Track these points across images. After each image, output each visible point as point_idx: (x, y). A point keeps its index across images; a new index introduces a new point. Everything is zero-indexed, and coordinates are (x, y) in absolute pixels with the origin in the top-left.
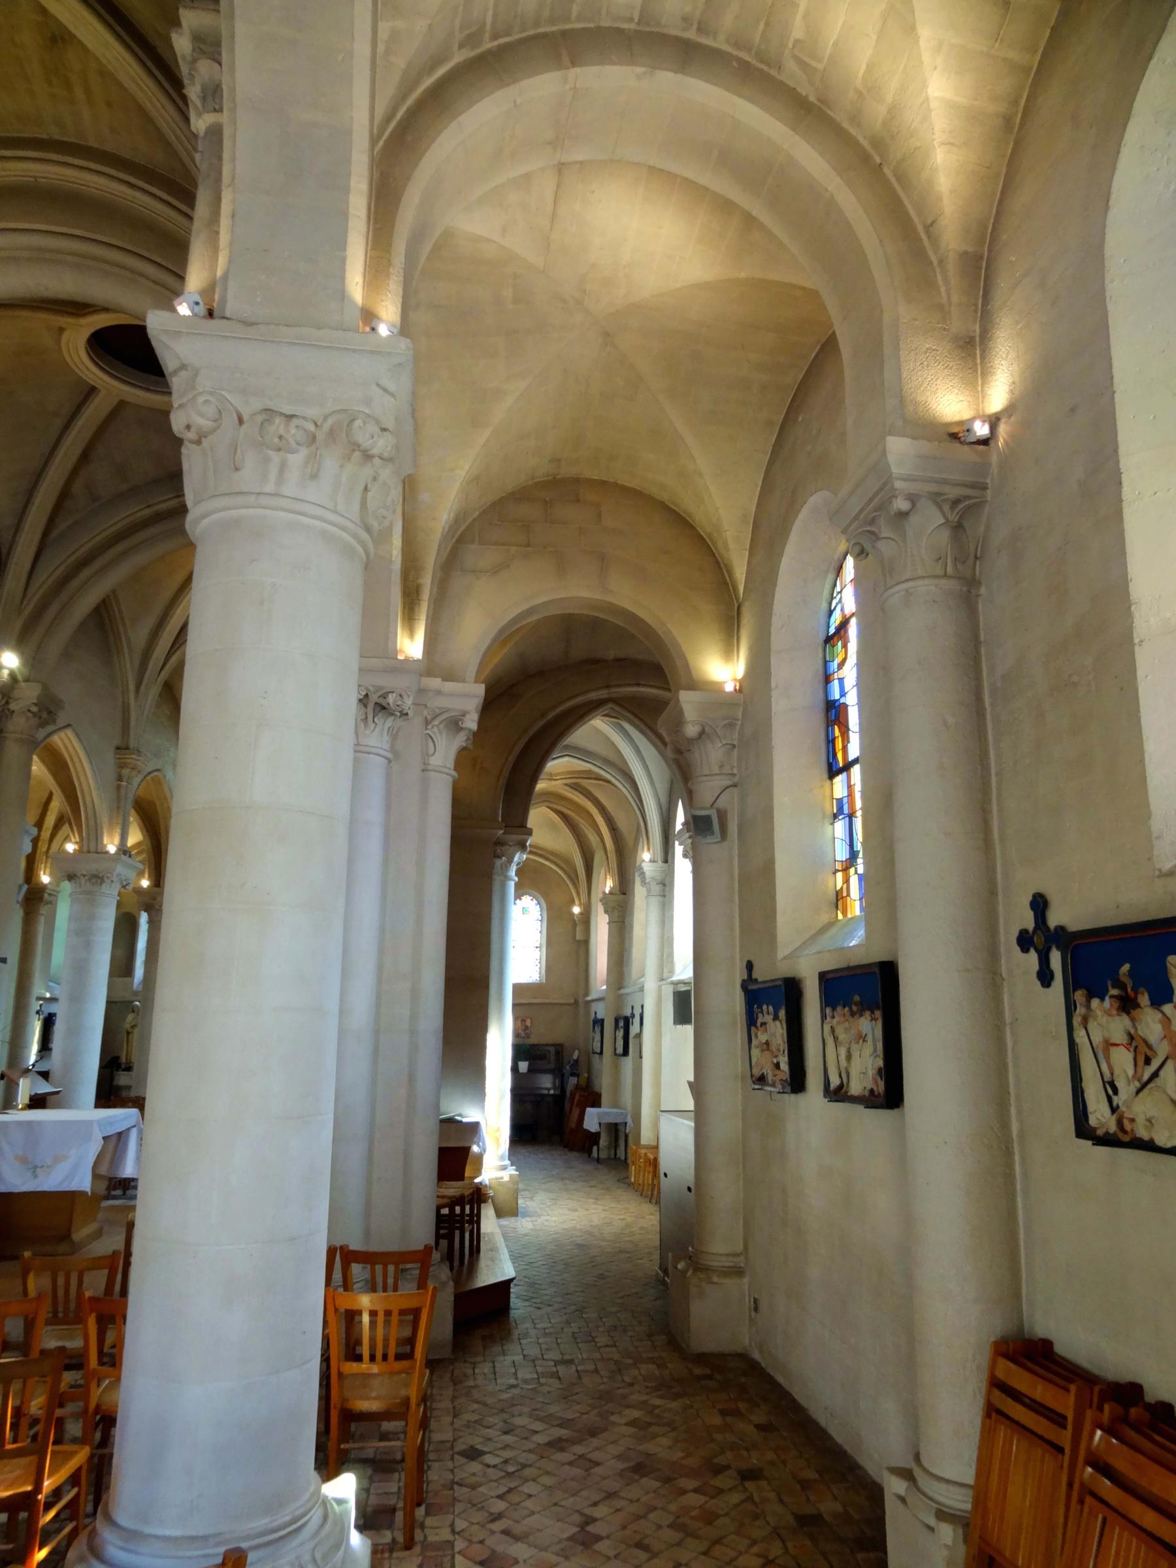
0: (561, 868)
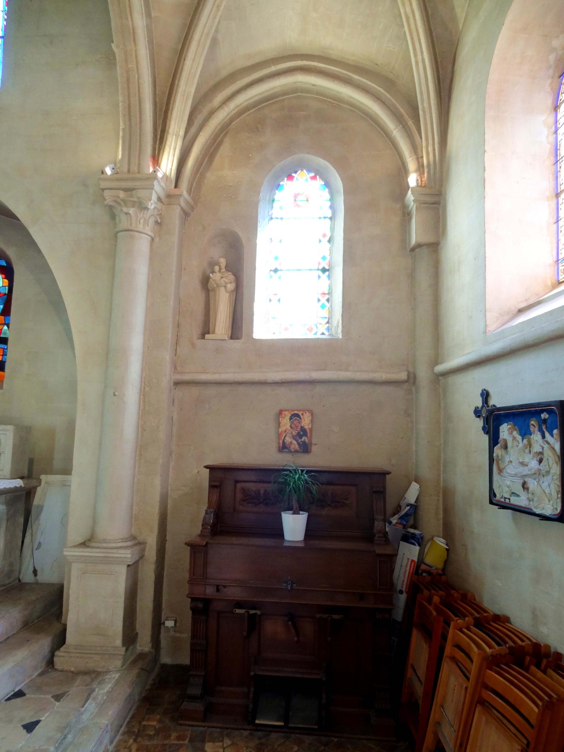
0: (377, 98)
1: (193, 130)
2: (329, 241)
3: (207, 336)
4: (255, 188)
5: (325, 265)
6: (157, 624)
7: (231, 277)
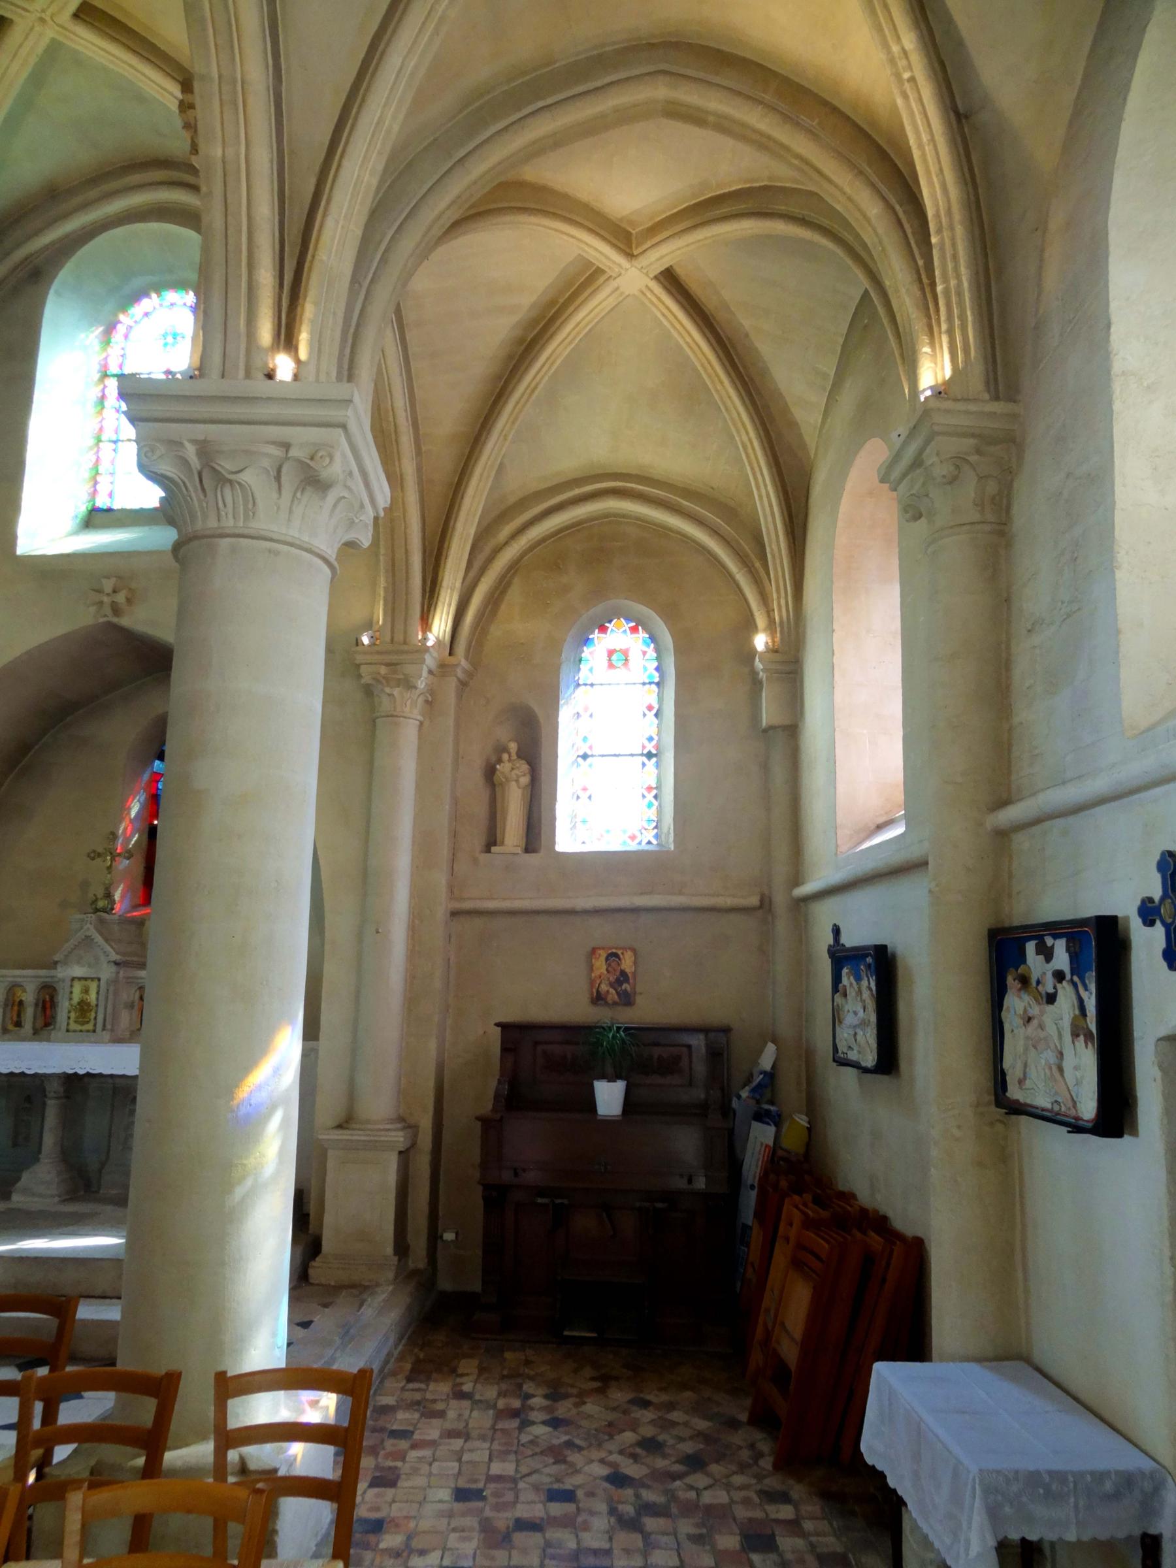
0: (715, 532)
1: (472, 574)
2: (656, 715)
3: (493, 849)
4: (554, 647)
5: (650, 747)
6: (434, 1237)
7: (525, 767)
